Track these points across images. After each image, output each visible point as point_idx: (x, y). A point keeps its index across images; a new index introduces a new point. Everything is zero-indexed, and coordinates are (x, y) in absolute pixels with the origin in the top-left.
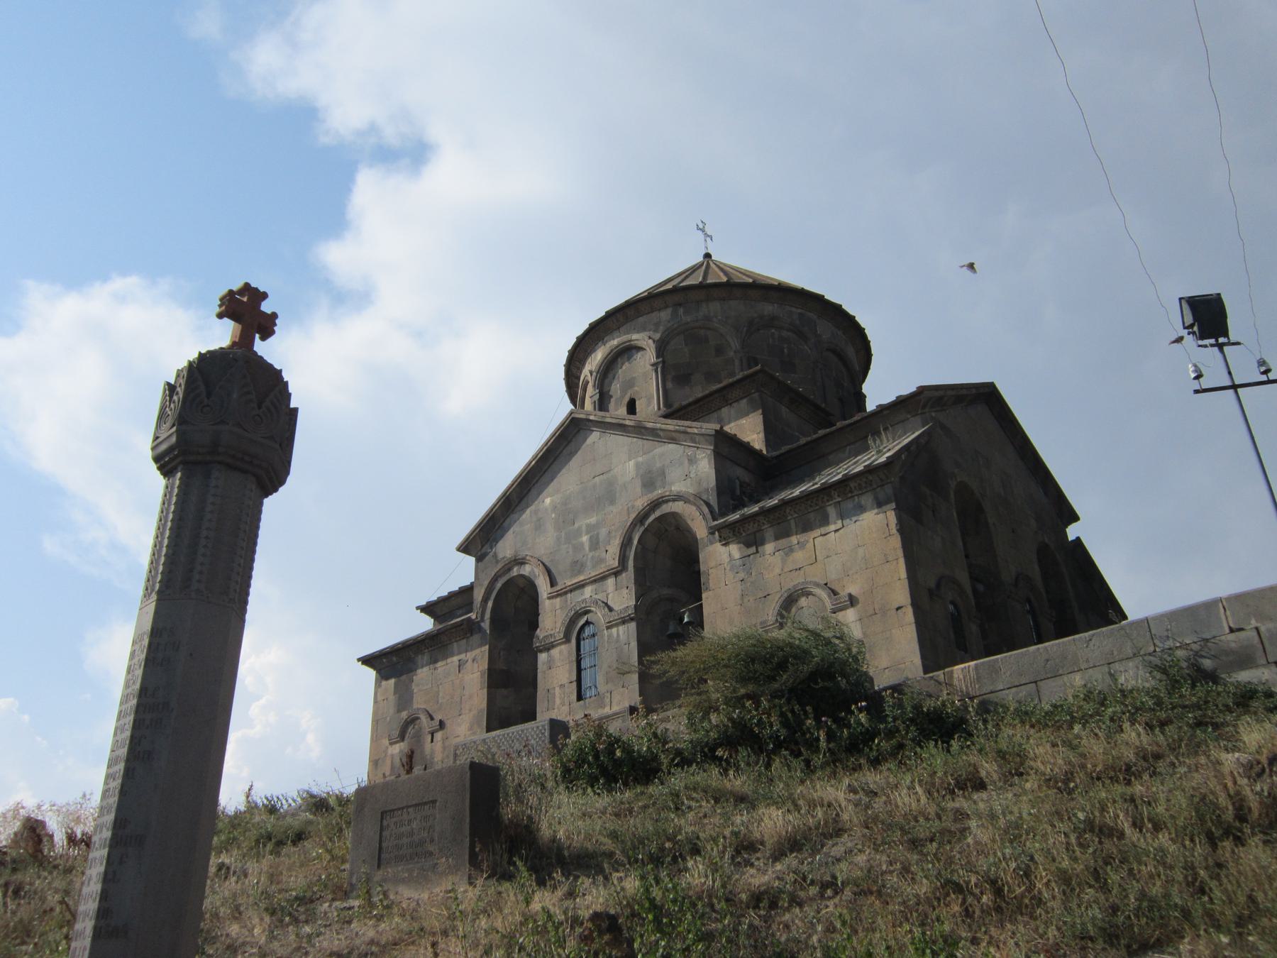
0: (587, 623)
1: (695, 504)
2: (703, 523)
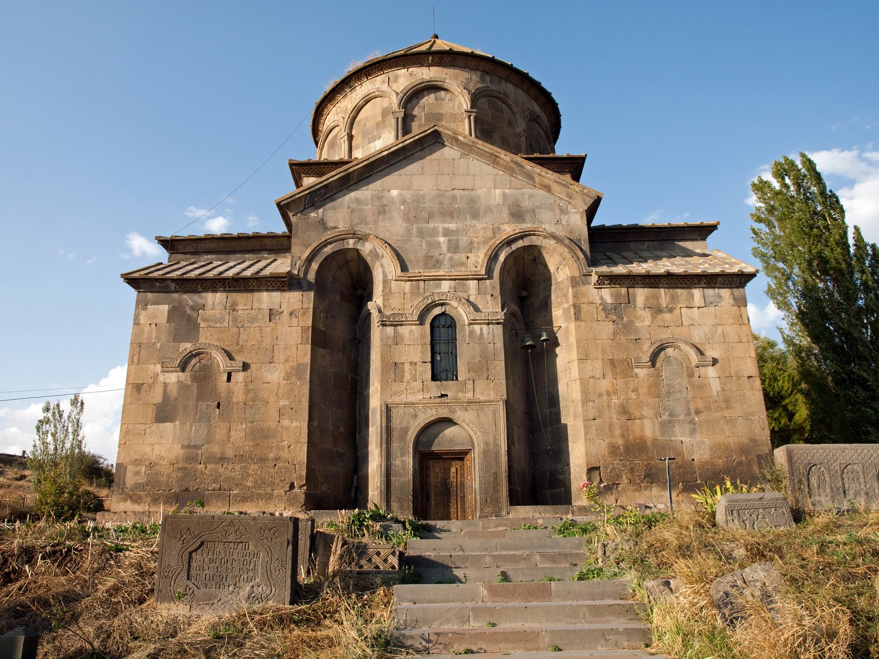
0: (443, 314)
1: (567, 246)
2: (575, 265)
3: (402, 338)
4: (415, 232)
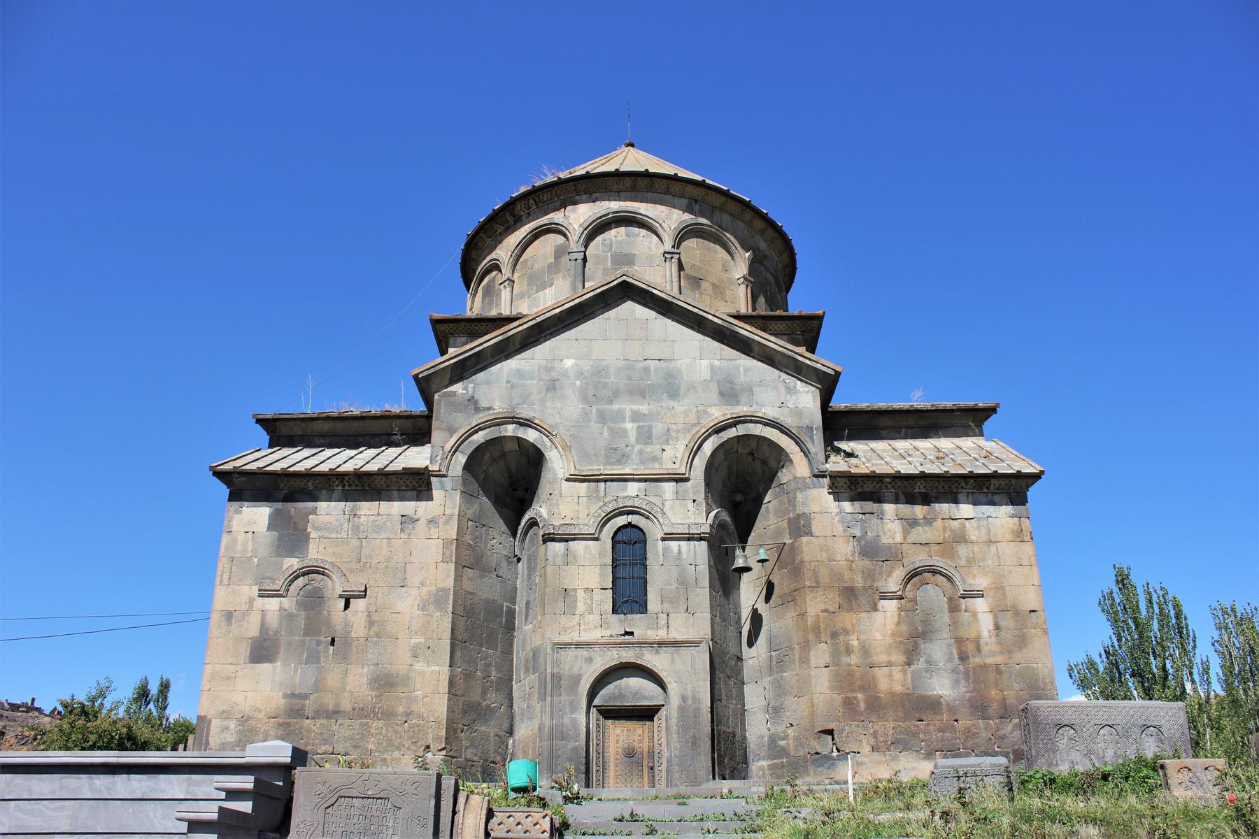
3: (575, 556)
4: (594, 416)
